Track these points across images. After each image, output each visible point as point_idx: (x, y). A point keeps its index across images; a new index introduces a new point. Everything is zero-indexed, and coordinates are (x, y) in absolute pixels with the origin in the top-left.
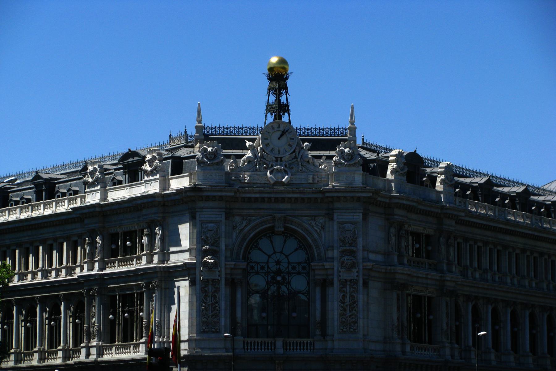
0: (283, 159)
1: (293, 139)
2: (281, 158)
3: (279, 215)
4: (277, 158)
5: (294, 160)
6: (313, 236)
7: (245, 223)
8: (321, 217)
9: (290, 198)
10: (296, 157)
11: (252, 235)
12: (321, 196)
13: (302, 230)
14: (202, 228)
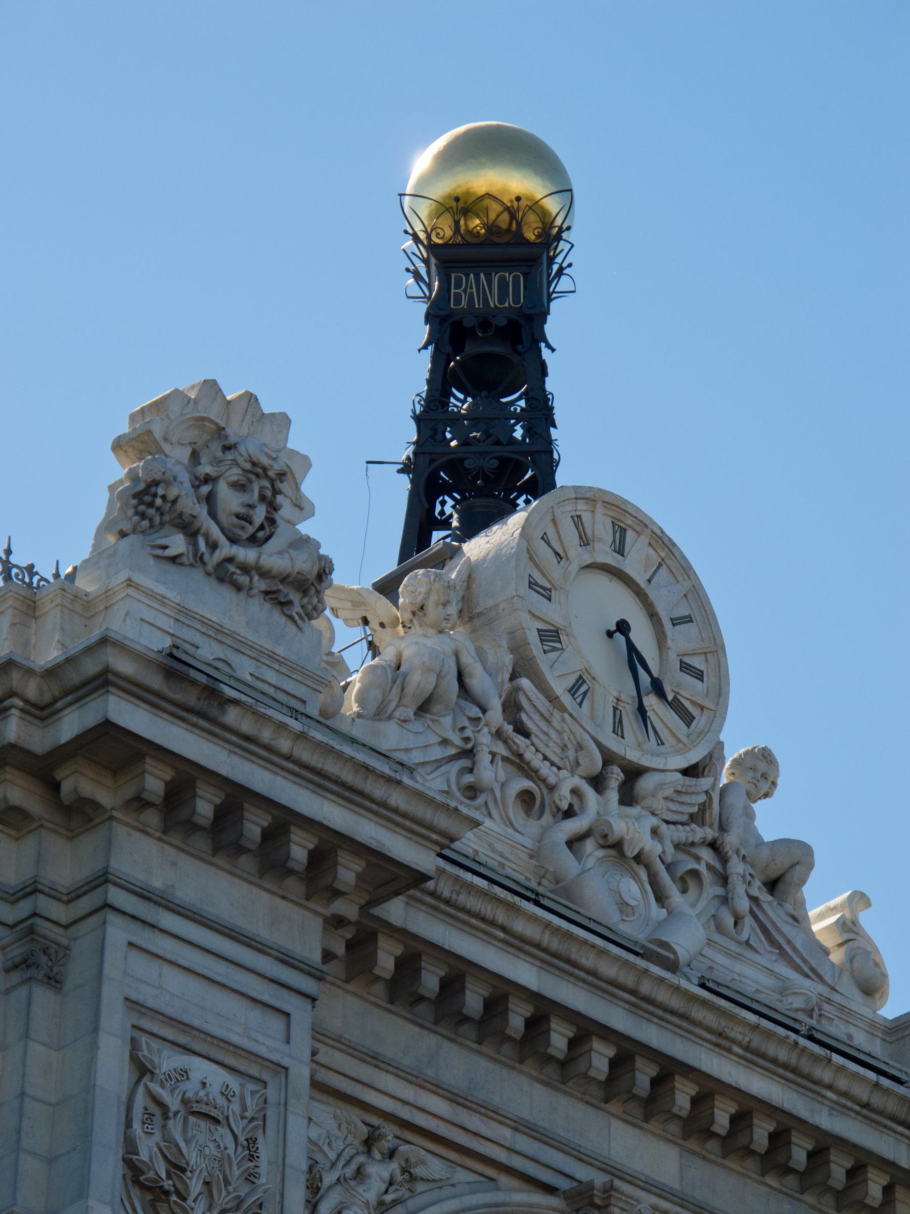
0: (646, 784)
2: (634, 773)
4: (609, 758)
5: (700, 833)
7: (379, 1172)
9: (709, 1089)
10: (698, 818)
14: (142, 1069)
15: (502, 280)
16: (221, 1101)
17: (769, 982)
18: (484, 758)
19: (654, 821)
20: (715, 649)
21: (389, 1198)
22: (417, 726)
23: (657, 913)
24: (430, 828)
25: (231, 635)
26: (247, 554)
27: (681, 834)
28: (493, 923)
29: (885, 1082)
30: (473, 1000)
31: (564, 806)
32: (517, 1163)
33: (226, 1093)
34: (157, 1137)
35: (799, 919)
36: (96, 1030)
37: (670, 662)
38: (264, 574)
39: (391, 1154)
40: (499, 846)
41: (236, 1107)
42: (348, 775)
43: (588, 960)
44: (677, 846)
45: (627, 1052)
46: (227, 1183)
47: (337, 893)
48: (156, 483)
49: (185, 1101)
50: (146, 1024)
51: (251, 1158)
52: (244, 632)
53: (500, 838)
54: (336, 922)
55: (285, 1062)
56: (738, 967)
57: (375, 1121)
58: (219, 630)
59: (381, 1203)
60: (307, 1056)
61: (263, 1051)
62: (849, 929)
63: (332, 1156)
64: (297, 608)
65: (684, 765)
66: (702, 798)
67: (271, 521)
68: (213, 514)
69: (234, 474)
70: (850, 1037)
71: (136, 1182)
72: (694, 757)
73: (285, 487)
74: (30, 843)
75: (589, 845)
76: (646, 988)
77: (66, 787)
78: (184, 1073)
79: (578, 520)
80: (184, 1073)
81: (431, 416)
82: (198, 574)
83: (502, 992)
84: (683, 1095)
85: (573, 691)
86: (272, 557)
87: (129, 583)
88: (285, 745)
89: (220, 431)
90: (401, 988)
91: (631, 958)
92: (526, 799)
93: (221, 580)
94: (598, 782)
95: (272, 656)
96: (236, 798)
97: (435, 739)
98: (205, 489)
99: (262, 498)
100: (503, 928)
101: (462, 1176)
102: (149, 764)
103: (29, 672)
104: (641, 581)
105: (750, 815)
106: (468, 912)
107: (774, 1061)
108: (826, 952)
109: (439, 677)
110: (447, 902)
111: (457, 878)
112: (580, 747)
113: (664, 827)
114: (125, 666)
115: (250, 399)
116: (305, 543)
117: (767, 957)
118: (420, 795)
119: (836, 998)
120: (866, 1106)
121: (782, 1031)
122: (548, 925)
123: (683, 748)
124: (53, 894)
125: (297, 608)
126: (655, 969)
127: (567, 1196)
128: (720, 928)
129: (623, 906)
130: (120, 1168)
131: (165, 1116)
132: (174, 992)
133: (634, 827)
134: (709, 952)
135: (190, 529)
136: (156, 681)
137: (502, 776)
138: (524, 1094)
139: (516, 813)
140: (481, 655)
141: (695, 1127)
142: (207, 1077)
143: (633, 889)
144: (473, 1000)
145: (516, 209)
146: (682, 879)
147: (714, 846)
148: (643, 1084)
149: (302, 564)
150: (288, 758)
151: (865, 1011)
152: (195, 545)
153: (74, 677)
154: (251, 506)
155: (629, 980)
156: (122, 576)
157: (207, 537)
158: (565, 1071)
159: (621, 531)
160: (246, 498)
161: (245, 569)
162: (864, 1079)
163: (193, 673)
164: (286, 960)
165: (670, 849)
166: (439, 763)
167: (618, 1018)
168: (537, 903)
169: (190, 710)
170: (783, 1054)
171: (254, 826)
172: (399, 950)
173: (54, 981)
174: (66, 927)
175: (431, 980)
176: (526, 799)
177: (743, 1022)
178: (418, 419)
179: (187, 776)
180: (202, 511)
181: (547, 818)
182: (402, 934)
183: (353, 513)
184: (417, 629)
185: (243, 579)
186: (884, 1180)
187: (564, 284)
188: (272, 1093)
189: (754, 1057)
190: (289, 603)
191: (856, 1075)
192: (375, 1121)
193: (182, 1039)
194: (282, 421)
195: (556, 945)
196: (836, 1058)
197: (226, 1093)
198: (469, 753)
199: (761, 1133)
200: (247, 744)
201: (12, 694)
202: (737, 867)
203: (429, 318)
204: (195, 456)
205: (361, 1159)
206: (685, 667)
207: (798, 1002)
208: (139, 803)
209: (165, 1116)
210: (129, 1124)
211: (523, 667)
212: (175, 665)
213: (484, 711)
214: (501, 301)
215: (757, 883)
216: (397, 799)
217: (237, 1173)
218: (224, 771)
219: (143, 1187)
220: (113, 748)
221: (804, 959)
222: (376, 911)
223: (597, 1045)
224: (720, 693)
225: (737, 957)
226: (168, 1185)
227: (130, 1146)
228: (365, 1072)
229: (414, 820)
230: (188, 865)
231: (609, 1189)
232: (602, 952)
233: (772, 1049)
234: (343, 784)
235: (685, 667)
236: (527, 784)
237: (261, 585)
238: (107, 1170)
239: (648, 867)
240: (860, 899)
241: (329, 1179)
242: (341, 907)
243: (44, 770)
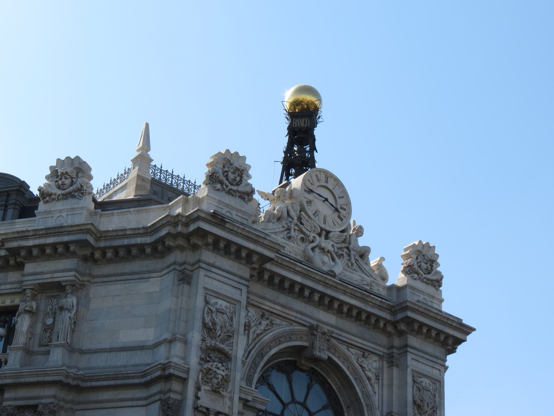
0: (331, 235)
1: (345, 210)
2: (328, 232)
3: (326, 328)
4: (322, 229)
5: (344, 245)
6: (364, 387)
8: (376, 358)
9: (342, 303)
10: (344, 242)
11: (274, 351)
12: (386, 315)
13: (348, 368)
14: (207, 302)
15: (305, 121)
16: (225, 309)
17: (360, 278)
18: (292, 230)
19: (332, 243)
20: (349, 204)
21: (266, 328)
22: (277, 223)
23: (332, 263)
24: (274, 248)
25: (231, 206)
26: (235, 188)
27: (339, 246)
28: (291, 268)
29: (383, 301)
30: (287, 285)
31: (311, 240)
32: (297, 320)
33: (226, 307)
34: (210, 317)
35: (368, 263)
36: (197, 294)
37: (341, 206)
38: (239, 192)
39: (268, 319)
40: (296, 250)
41: (228, 310)
42: (254, 237)
43: (313, 275)
44: (338, 248)
45: (323, 295)
46: (225, 327)
47: (253, 263)
48: (213, 173)
49: (216, 309)
50: (208, 292)
51: (232, 321)
52: (233, 205)
53: (294, 249)
54: (254, 269)
55: (240, 300)
56: (352, 275)
57: (264, 311)
58: (228, 205)
59: (265, 330)
60: (245, 298)
61: (235, 298)
62: (380, 266)
63: (254, 319)
64: (247, 199)
65: (340, 230)
66: (345, 237)
67: (241, 180)
68: (227, 179)
69: (232, 170)
70: (378, 290)
71: (205, 327)
72: (342, 228)
73: (245, 172)
74: (184, 253)
75: (317, 249)
76: (327, 281)
77: (191, 241)
78: (217, 303)
79: (317, 176)
80: (217, 303)
81: (289, 150)
82: (224, 193)
83: (293, 283)
84: (336, 305)
85: (314, 215)
86: (241, 188)
87: (207, 195)
88: (240, 231)
89: (229, 161)
90: (270, 283)
91: (323, 275)
92: (302, 239)
93: (229, 194)
94: (320, 235)
95: (240, 210)
96: (229, 243)
97: (281, 226)
98: (226, 174)
99: (238, 175)
100: (293, 269)
101: (284, 323)
102: (209, 236)
103: (183, 216)
104: (331, 189)
105: (357, 241)
106: (285, 266)
107: (357, 297)
108: (374, 271)
109: (282, 212)
110: (280, 263)
111: (282, 258)
112: (315, 227)
113: (335, 244)
114: (203, 215)
115: (237, 153)
116: (249, 185)
117: (360, 273)
118: (271, 241)
119: (376, 281)
120: (379, 306)
121: (359, 290)
122: (303, 268)
123: (340, 226)
124: (189, 264)
125: (247, 199)
126: (329, 277)
127: (308, 327)
128: (348, 267)
129: (324, 263)
130: (201, 324)
131: (212, 313)
132: (215, 285)
133: (327, 245)
134: (344, 272)
135: (222, 183)
136: (210, 218)
137: (297, 234)
138: (299, 305)
139: (300, 242)
140: (293, 208)
141: (339, 312)
142: (222, 304)
143: (326, 259)
144: (287, 285)
145: (309, 104)
146: (339, 256)
147: (347, 248)
148: (327, 303)
149: (247, 189)
150: (241, 234)
151: (383, 284)
152: (223, 186)
153: (192, 217)
154: (236, 177)
155: (323, 280)
156: (206, 194)
157: (226, 185)
158: (309, 300)
159: (327, 178)
160: (234, 175)
161: (234, 191)
162: (378, 300)
163: (218, 216)
164: (241, 277)
165: (336, 249)
166: (282, 232)
167: (320, 288)
168: (301, 263)
169: (218, 224)
170: (359, 295)
171: (233, 249)
172: (269, 274)
173: (189, 283)
174: (192, 271)
175: (277, 281)
176: (302, 239)
177: (350, 288)
178: (285, 152)
179: (217, 239)
180: (224, 179)
181: (307, 243)
182: (270, 271)
183: (265, 175)
184: (278, 202)
185: (234, 194)
186: (384, 322)
187: (320, 120)
188: (237, 307)
189: (352, 296)
190: (245, 198)
191: (376, 299)
192: (264, 311)
193: (217, 296)
194: (244, 158)
195: (305, 272)
196: (372, 296)
197: (226, 307)
198: (289, 229)
199: (354, 313)
200: (231, 231)
201: (179, 221)
202: (352, 253)
203: (288, 129)
204: (224, 167)
205: (261, 320)
206: (342, 208)
207: (365, 283)
208: (207, 244)
209: (212, 313)
210: (204, 314)
211: (302, 209)
212: (215, 215)
213: (293, 219)
214: (305, 124)
215: (357, 256)
216: (266, 242)
217: (228, 325)
218: (226, 237)
219: (206, 328)
220: (200, 232)
221: (368, 272)
222: (263, 266)
223: (316, 294)
224: (350, 213)
225: (352, 273)
226: (212, 327)
227: (204, 319)
228: (262, 301)
229: (270, 247)
230: (219, 257)
231: (317, 326)
232: (316, 274)
233: (357, 294)
234: (253, 239)
235: (342, 208)
236: (303, 236)
237: (238, 194)
238: (198, 324)
239: (331, 254)
240: (382, 259)
241: (252, 324)
242: (254, 265)
243: (187, 237)
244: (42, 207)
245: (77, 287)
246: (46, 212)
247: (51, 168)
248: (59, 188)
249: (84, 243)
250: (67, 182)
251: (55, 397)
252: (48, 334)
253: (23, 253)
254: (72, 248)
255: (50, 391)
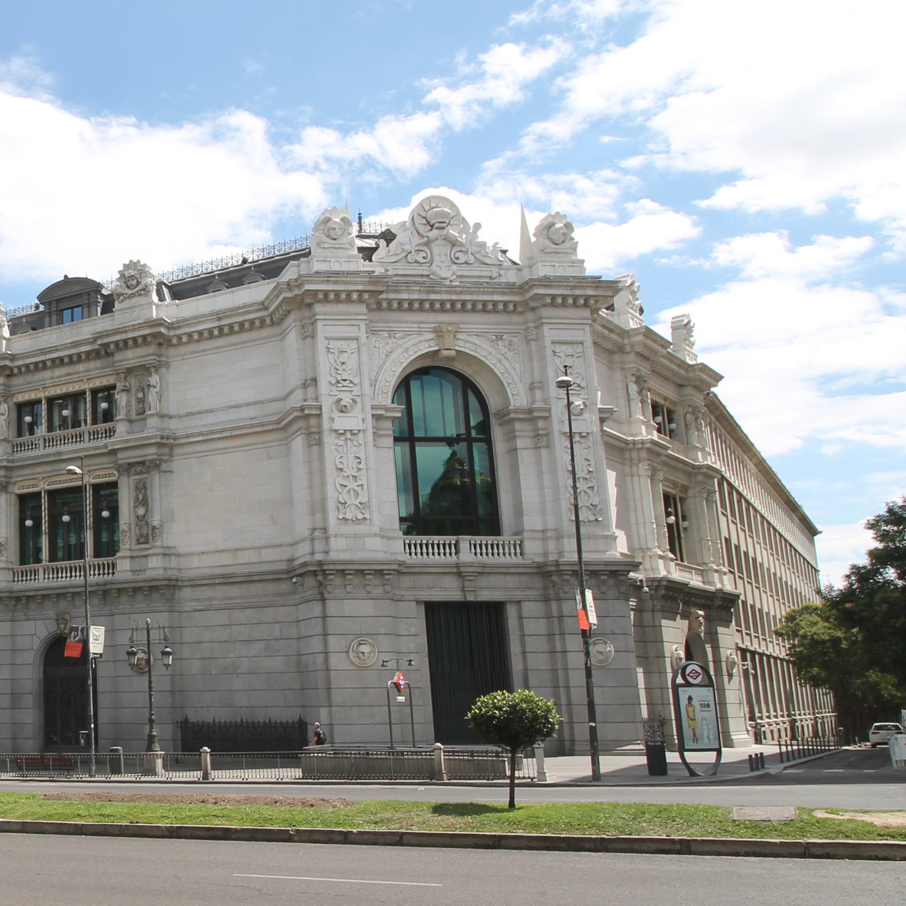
244: (117, 305)
245: (157, 368)
246: (121, 310)
247: (120, 272)
248: (128, 287)
249: (155, 335)
250: (134, 282)
251: (156, 454)
252: (141, 406)
253: (112, 347)
254: (149, 339)
255: (153, 450)
